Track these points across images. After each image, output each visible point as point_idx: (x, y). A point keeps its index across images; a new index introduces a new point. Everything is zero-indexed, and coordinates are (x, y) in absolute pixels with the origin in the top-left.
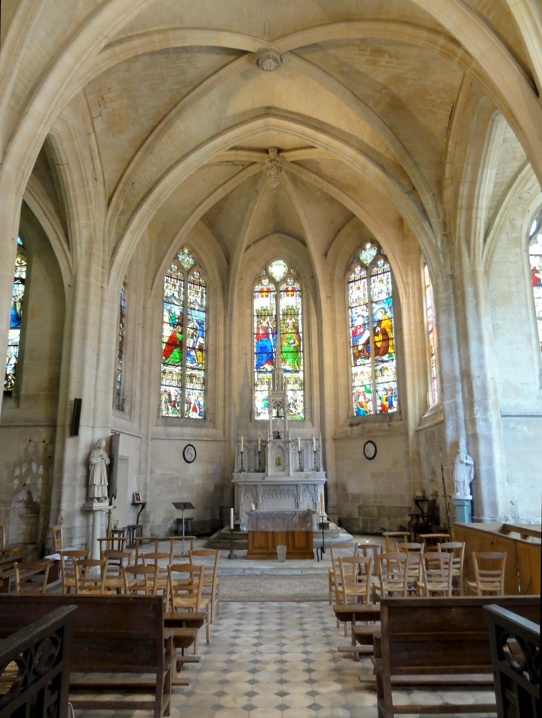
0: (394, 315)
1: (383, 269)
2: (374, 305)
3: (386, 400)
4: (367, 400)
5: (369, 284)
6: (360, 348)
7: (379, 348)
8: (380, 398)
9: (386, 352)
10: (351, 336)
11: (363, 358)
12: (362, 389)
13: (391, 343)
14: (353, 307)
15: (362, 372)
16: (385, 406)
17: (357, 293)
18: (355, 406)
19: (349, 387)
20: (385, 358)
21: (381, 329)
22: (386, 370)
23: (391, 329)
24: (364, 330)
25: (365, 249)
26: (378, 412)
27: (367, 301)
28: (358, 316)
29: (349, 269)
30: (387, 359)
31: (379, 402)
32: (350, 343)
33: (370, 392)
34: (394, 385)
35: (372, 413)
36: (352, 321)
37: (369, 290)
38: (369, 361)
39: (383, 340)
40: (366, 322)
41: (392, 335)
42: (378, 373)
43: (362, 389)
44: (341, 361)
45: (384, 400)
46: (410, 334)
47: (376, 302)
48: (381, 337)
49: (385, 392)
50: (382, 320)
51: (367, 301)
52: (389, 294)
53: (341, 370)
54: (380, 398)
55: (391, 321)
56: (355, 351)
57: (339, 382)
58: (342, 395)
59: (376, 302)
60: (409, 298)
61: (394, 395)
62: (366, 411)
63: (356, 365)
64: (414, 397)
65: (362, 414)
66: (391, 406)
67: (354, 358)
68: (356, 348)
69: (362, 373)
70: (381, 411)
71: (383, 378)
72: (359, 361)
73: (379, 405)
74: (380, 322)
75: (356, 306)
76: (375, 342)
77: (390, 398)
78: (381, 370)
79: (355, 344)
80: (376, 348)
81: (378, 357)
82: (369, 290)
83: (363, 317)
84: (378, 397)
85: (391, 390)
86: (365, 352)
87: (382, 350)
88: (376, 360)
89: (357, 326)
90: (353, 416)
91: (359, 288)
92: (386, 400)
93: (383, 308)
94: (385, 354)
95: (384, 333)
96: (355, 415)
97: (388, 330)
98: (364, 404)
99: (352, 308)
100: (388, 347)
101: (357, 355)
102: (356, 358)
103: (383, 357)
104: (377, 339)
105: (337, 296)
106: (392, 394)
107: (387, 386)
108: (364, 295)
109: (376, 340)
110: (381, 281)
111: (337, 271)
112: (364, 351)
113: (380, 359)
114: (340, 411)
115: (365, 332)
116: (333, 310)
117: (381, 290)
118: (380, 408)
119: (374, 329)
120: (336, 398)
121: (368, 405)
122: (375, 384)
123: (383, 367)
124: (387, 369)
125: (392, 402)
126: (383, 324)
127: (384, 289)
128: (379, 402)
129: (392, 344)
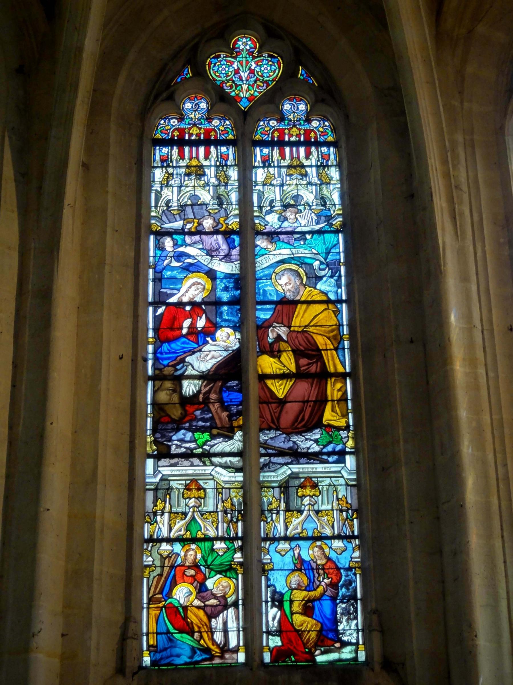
0: (349, 293)
1: (307, 132)
2: (261, 242)
3: (308, 609)
4: (213, 602)
5: (245, 167)
6: (189, 387)
7: (282, 402)
8: (278, 600)
9: (310, 420)
10: (151, 334)
11: (203, 430)
12: (193, 553)
13: (333, 389)
14: (169, 233)
15: (195, 486)
16: (299, 633)
17: (183, 185)
18: (148, 620)
19: (132, 542)
20: (308, 442)
21: (290, 333)
22: (308, 491)
23: (338, 339)
24: (216, 327)
25: (233, 52)
26: (267, 658)
27: (233, 223)
28: (189, 269)
29: (163, 95)
30: (316, 448)
31: (272, 615)
32: (146, 360)
33: (227, 570)
34: (347, 554)
35: (241, 657)
36: (158, 280)
37: (246, 185)
38: (235, 443)
39: (298, 375)
40: (225, 297)
41: (338, 362)
42: (270, 497)
43: (193, 553)
44: (110, 425)
45: (296, 607)
46: (471, 362)
47: (272, 236)
48: (288, 362)
49: (295, 579)
50: (295, 303)
51: (233, 223)
52: (329, 218)
53: (109, 463)
54: (278, 600)
55: (337, 313)
56: (163, 397)
57: (98, 512)
58: (105, 566)
59: (272, 236)
60: (464, 238)
61: (343, 591)
62: (207, 650)
63: (163, 454)
64: (494, 607)
65: (184, 659)
66: (329, 636)
67: (155, 423)
68: (168, 384)
69: (193, 486)
70: (278, 654)
71: (296, 521)
72: (181, 440)
73: (274, 625)
74: (286, 306)
75: (182, 232)
76: (263, 377)
77: (327, 605)
78: (285, 487)
79: (168, 371)
80: (268, 398)
81: (272, 434)
82: (246, 185)
83: (211, 274)
84: (266, 594)
85: (332, 568)
86: (215, 407)
87: (291, 410)
88: (265, 445)
89: (180, 304)
90: (141, 668)
91: (198, 172)
92: (308, 609)
93: (301, 262)
94: (309, 429)
95: (307, 350)
96: (147, 660)
97: (321, 341)
98: (195, 617)
99: (161, 234)
100: (322, 401)
101: (176, 413)
102: (166, 422)
103: (294, 438)
104: (267, 364)
105: (114, 169)
106: (334, 585)
107: (308, 552)
108: (220, 200)
109: (268, 371)
110: (297, 167)
111: (121, 80)
112: (207, 401)
113: (281, 442)
114: (94, 634)
115: (220, 334)
116: (93, 215)
117: (297, 197)
118: (275, 642)
119: (263, 327)
120: (78, 575)
121: (217, 623)
122: (250, 543)
123: (294, 476)
124: (315, 486)
125: (336, 622)
126: (302, 318)
127: (309, 196)
128: (272, 615)
129: (337, 395)
